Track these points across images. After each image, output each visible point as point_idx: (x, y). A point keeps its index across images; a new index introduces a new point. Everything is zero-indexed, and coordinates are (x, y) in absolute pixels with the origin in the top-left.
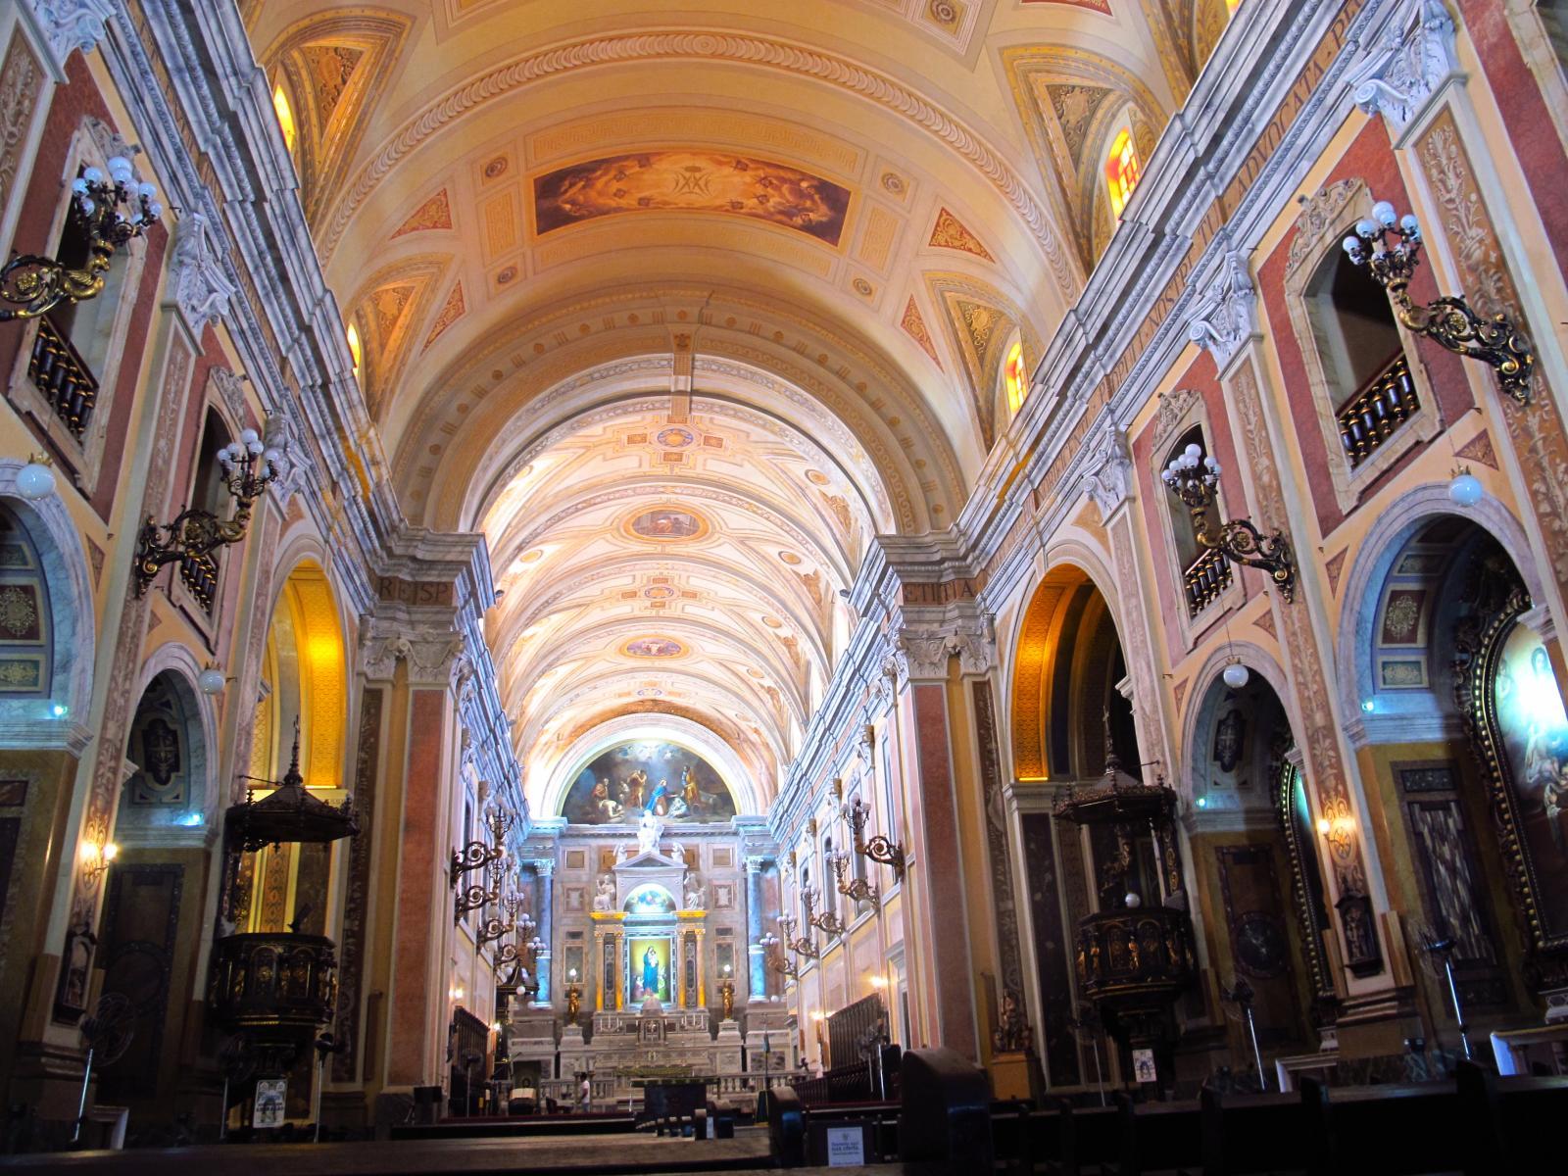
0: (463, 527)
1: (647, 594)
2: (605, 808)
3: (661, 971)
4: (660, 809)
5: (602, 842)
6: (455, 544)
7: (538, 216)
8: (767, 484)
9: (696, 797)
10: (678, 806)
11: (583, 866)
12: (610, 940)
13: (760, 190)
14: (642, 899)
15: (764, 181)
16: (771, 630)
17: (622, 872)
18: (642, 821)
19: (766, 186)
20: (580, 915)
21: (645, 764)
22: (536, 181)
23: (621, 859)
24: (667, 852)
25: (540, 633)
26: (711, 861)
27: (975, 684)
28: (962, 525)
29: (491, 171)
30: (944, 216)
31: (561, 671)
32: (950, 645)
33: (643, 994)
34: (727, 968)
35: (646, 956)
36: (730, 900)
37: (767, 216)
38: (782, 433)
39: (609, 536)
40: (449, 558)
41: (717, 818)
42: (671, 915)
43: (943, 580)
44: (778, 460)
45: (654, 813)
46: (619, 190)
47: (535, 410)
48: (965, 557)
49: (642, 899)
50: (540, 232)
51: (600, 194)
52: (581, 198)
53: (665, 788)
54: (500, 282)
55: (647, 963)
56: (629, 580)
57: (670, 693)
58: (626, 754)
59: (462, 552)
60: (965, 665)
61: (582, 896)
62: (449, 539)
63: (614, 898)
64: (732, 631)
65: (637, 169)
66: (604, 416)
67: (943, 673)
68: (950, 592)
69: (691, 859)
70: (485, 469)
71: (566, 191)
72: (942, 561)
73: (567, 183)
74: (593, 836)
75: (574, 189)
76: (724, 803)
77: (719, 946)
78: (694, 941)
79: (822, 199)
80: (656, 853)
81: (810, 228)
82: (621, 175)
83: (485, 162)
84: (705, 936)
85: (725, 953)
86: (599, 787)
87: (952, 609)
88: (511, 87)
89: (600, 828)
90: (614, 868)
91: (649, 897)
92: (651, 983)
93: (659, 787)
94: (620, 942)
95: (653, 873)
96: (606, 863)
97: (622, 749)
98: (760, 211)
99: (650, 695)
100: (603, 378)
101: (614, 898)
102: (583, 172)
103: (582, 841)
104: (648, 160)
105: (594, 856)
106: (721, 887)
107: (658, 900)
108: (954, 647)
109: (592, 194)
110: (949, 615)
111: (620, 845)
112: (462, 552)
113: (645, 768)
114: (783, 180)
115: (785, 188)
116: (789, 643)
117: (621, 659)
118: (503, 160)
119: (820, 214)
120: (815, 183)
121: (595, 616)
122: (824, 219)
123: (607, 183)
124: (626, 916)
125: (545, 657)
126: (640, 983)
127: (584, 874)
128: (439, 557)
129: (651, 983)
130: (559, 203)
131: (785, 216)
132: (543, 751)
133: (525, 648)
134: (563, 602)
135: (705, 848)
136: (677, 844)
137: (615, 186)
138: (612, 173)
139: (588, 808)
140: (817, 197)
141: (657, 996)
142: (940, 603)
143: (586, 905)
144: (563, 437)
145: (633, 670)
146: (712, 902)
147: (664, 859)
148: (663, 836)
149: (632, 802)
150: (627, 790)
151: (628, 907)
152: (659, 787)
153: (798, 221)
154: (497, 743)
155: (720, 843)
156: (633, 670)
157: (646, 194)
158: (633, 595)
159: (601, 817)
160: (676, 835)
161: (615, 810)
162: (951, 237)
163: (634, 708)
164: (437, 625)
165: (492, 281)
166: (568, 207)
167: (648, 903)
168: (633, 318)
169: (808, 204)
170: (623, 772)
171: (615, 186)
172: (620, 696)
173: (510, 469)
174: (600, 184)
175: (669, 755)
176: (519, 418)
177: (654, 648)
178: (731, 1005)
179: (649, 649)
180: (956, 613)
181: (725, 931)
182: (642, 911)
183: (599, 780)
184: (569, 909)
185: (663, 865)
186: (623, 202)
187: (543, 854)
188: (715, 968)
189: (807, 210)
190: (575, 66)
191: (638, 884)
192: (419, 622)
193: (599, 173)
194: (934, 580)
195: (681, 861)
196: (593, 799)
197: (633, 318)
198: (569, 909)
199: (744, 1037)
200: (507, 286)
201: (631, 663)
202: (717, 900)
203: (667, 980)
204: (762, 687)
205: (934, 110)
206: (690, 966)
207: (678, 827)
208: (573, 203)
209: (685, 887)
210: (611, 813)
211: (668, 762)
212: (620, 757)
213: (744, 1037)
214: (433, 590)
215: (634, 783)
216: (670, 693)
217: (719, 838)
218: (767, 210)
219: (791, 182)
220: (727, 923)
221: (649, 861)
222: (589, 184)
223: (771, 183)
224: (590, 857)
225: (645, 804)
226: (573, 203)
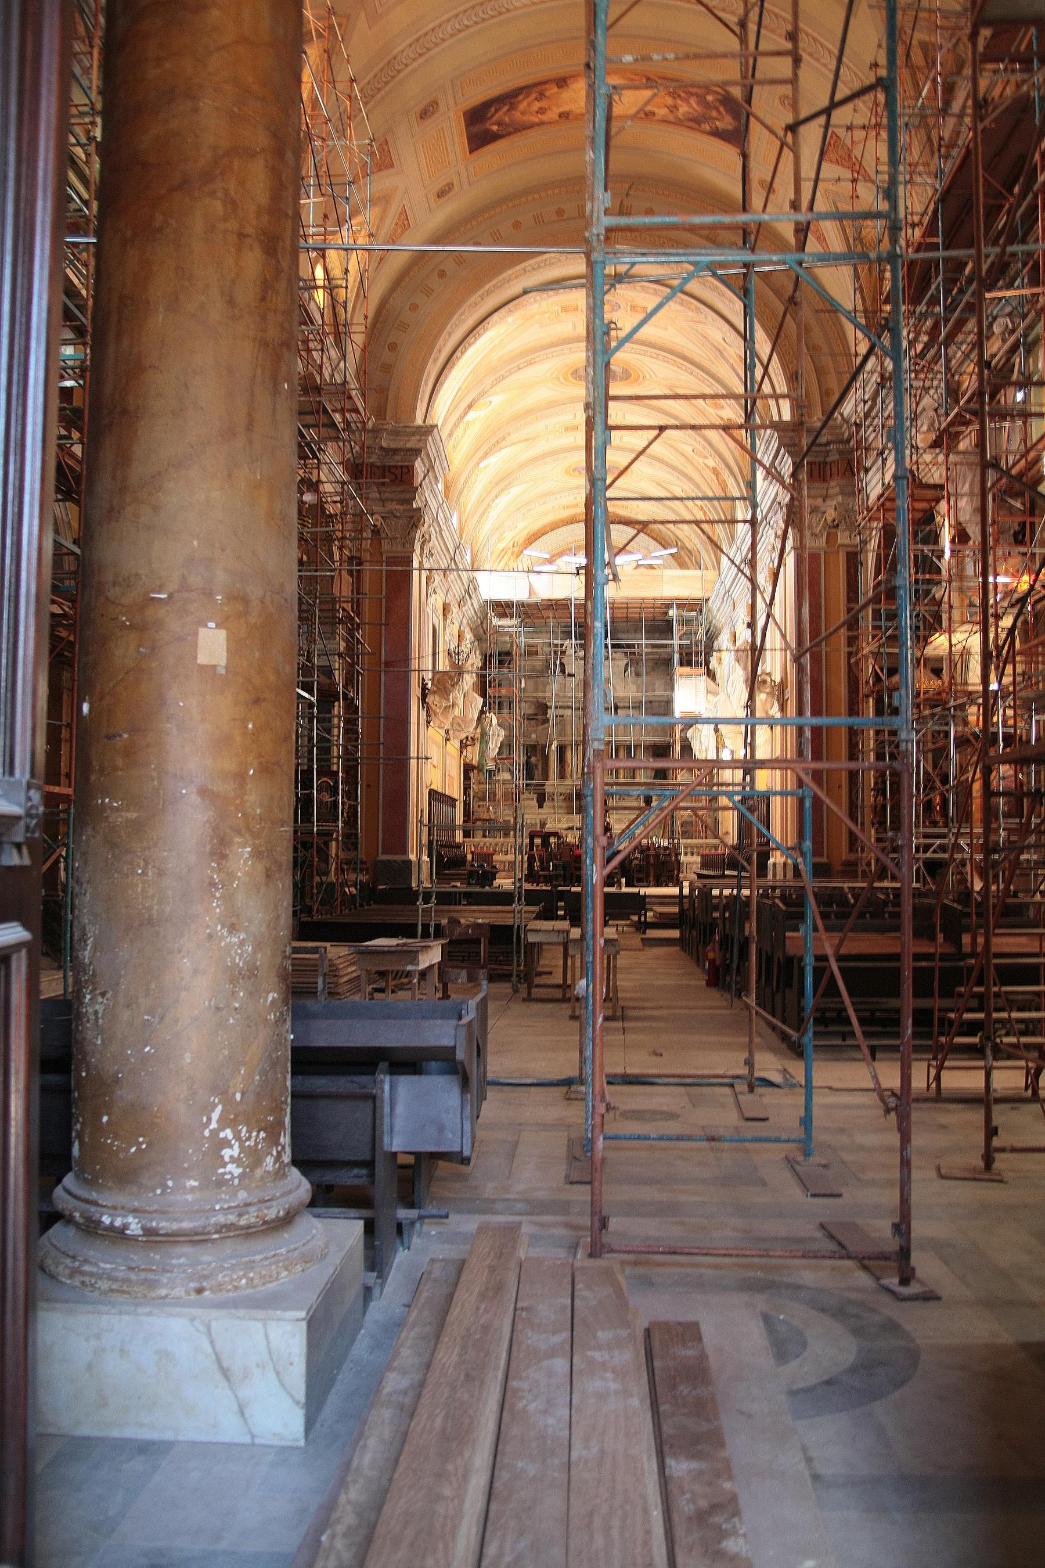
0: (419, 421)
6: (413, 434)
7: (468, 139)
8: (690, 346)
13: (670, 101)
15: (673, 95)
16: (700, 460)
19: (674, 98)
22: (464, 114)
25: (495, 463)
27: (848, 553)
28: (845, 415)
29: (425, 114)
30: (835, 137)
31: (515, 491)
32: (829, 519)
37: (678, 123)
38: (697, 310)
39: (550, 385)
40: (408, 446)
43: (829, 459)
44: (699, 327)
46: (541, 109)
47: (476, 304)
48: (848, 441)
50: (470, 152)
51: (523, 113)
52: (507, 119)
54: (439, 196)
56: (571, 416)
59: (420, 441)
60: (843, 538)
62: (408, 430)
64: (666, 459)
65: (556, 90)
66: (538, 298)
67: (822, 542)
68: (834, 470)
70: (435, 361)
71: (492, 116)
72: (828, 443)
73: (493, 110)
75: (500, 113)
79: (726, 111)
81: (716, 134)
82: (541, 95)
83: (419, 109)
87: (834, 486)
88: (436, 45)
98: (671, 118)
100: (534, 269)
102: (509, 98)
104: (565, 82)
108: (834, 521)
109: (517, 115)
110: (831, 491)
112: (420, 441)
114: (692, 94)
115: (693, 101)
116: (715, 472)
118: (434, 104)
119: (726, 122)
120: (720, 97)
121: (541, 447)
122: (730, 128)
123: (529, 105)
125: (497, 484)
128: (401, 445)
130: (487, 126)
131: (694, 122)
134: (514, 437)
137: (537, 105)
138: (533, 96)
140: (721, 109)
142: (824, 480)
144: (502, 319)
153: (706, 127)
157: (566, 108)
162: (841, 157)
164: (401, 502)
165: (432, 198)
166: (495, 128)
168: (560, 212)
169: (714, 114)
171: (537, 105)
173: (458, 353)
174: (523, 106)
176: (463, 313)
180: (837, 490)
186: (545, 118)
189: (715, 119)
190: (493, 17)
192: (387, 500)
193: (521, 97)
194: (821, 459)
197: (560, 212)
200: (445, 199)
205: (822, 45)
208: (499, 124)
214: (398, 472)
218: (677, 118)
219: (697, 95)
222: (513, 107)
223: (679, 96)
226: (499, 124)
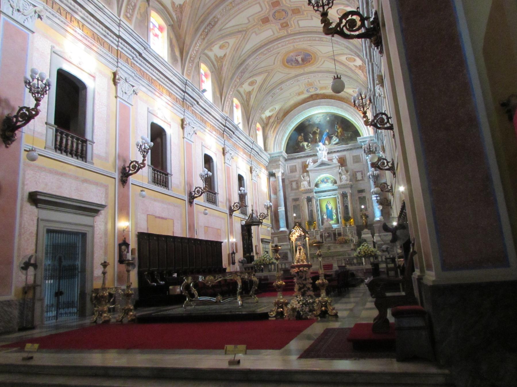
1: (274, 15)
2: (303, 146)
3: (334, 211)
4: (327, 142)
5: (303, 160)
9: (342, 134)
10: (335, 140)
11: (296, 171)
12: (309, 200)
14: (323, 181)
17: (311, 170)
18: (318, 149)
20: (297, 191)
21: (317, 124)
23: (311, 166)
24: (331, 160)
26: (352, 161)
33: (327, 221)
34: (363, 207)
35: (327, 205)
36: (362, 177)
41: (353, 142)
42: (335, 187)
45: (324, 144)
49: (323, 181)
53: (328, 133)
55: (327, 208)
57: (321, 88)
58: (310, 121)
61: (297, 183)
63: (309, 183)
69: (342, 162)
74: (298, 158)
76: (356, 133)
77: (360, 198)
78: (347, 197)
80: (325, 160)
84: (352, 195)
85: (362, 200)
86: (300, 137)
89: (301, 154)
90: (308, 169)
91: (325, 180)
92: (330, 217)
93: (325, 133)
94: (314, 201)
95: (325, 169)
96: (305, 167)
97: (308, 119)
99: (313, 92)
101: (309, 183)
103: (294, 161)
105: (301, 166)
106: (358, 172)
107: (330, 181)
111: (309, 160)
113: (319, 126)
117: (287, 70)
124: (316, 189)
126: (325, 217)
127: (297, 174)
129: (330, 217)
132: (272, 126)
133: (224, 63)
135: (348, 156)
136: (335, 156)
139: (297, 147)
141: (332, 222)
143: (298, 187)
145: (297, 76)
146: (354, 177)
147: (329, 162)
148: (328, 153)
149: (315, 142)
150: (311, 136)
151: (317, 185)
152: (325, 133)
154: (198, 103)
155: (355, 153)
156: (297, 76)
158: (265, 20)
159: (302, 149)
160: (335, 152)
161: (307, 146)
163: (308, 100)
167: (326, 183)
170: (309, 129)
172: (299, 94)
175: (328, 119)
177: (300, 60)
178: (366, 223)
179: (297, 61)
181: (361, 191)
182: (323, 186)
183: (300, 134)
184: (292, 189)
185: (329, 165)
187: (278, 167)
188: (359, 208)
191: (319, 175)
195: (337, 162)
196: (298, 143)
198: (292, 189)
199: (373, 237)
201: (294, 72)
202: (356, 178)
203: (337, 214)
204: (356, 66)
206: (346, 208)
207: (335, 148)
209: (340, 173)
210: (306, 148)
211: (328, 122)
212: (307, 123)
213: (373, 237)
215: (314, 133)
216: (321, 88)
217: (354, 151)
220: (362, 187)
221: (323, 164)
224: (299, 167)
225: (320, 141)
